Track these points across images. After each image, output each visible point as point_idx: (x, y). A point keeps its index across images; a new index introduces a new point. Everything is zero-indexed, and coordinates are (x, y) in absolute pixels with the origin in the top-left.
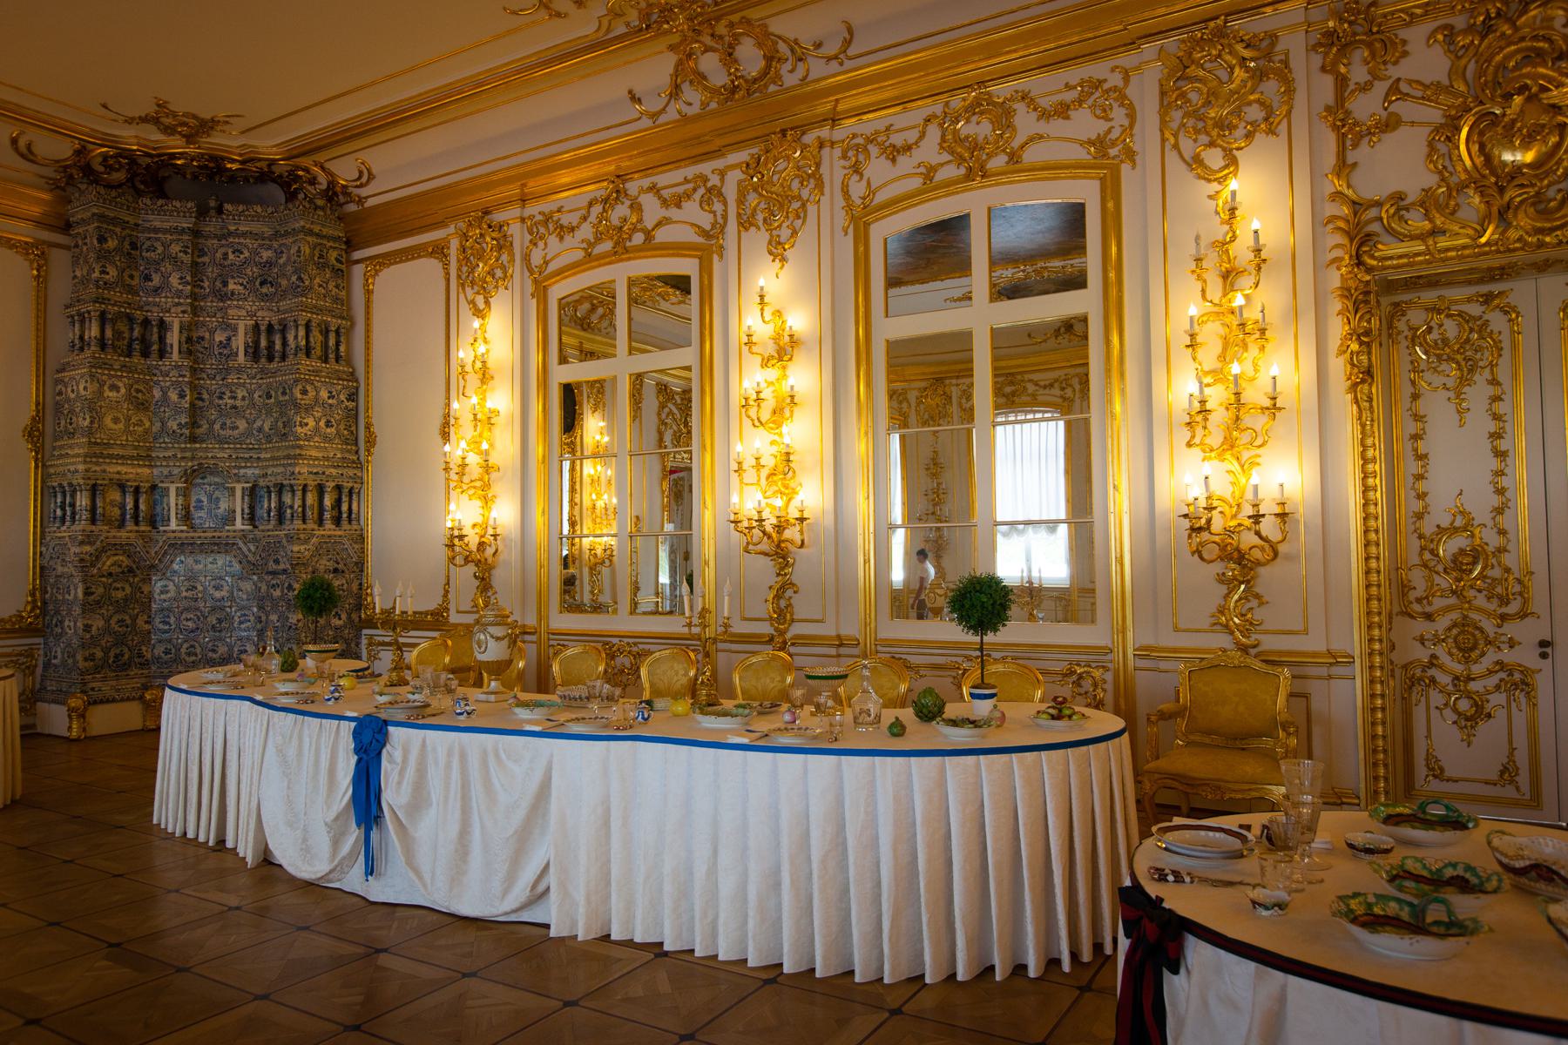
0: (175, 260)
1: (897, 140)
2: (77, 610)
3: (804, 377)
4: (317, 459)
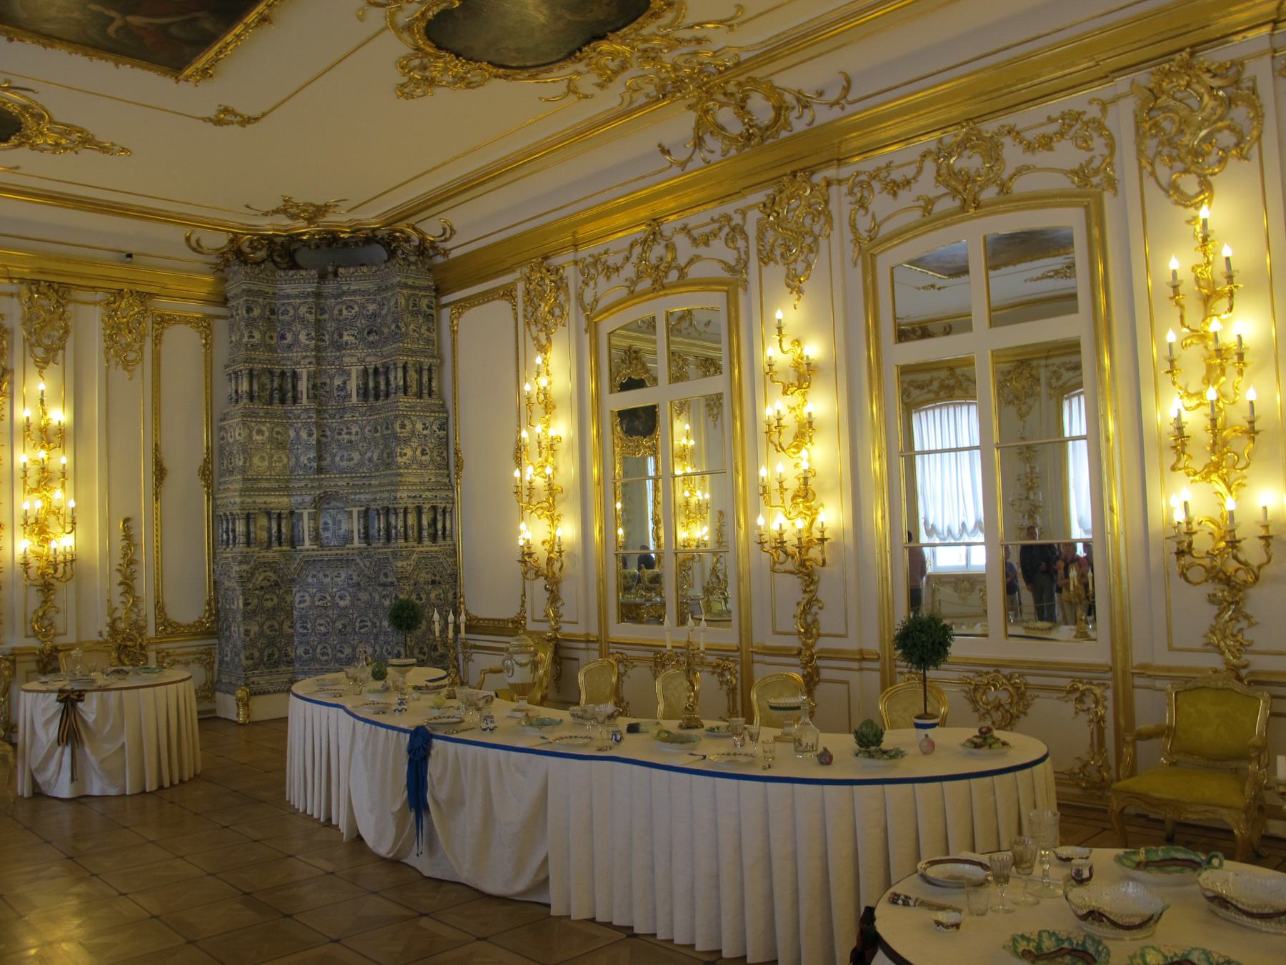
0: (303, 320)
1: (897, 175)
3: (821, 404)
4: (415, 484)
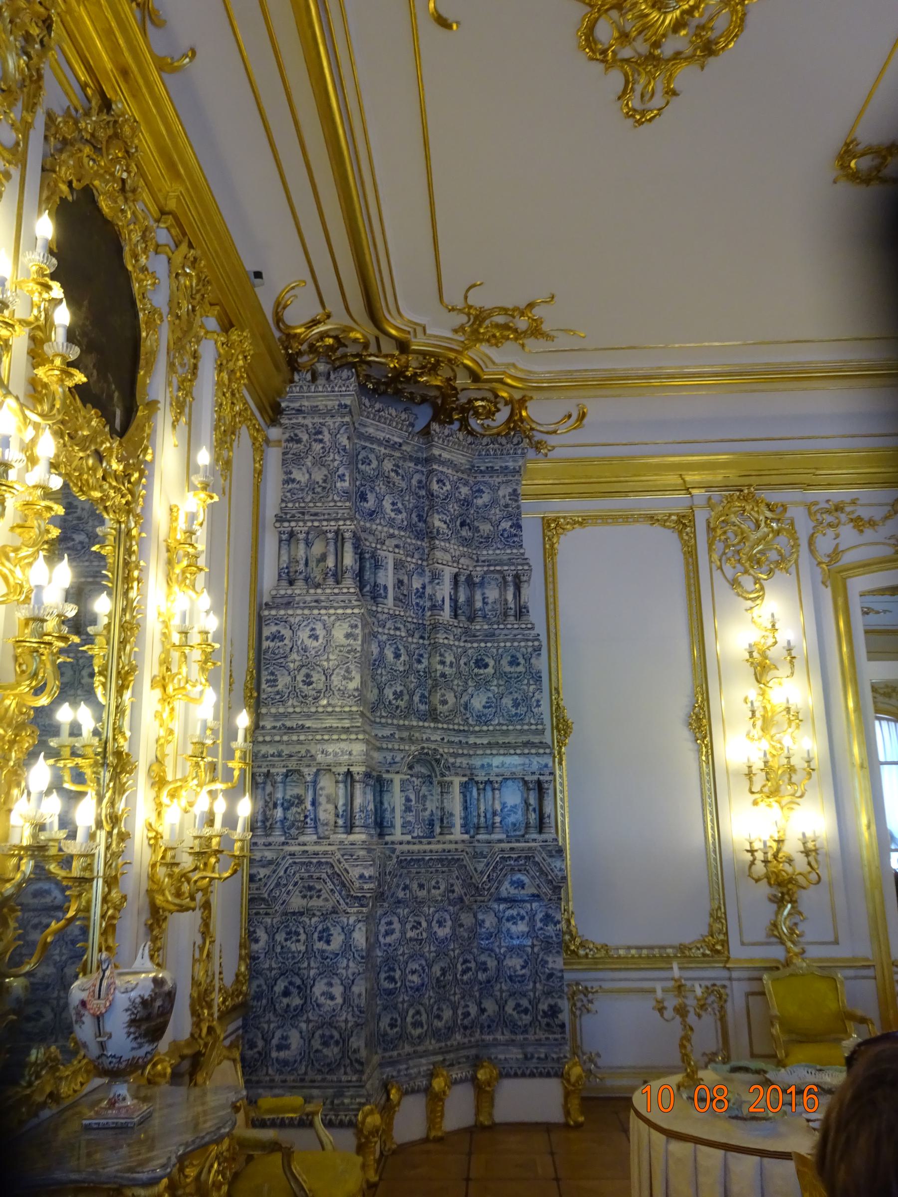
0: (388, 481)
2: (349, 967)
